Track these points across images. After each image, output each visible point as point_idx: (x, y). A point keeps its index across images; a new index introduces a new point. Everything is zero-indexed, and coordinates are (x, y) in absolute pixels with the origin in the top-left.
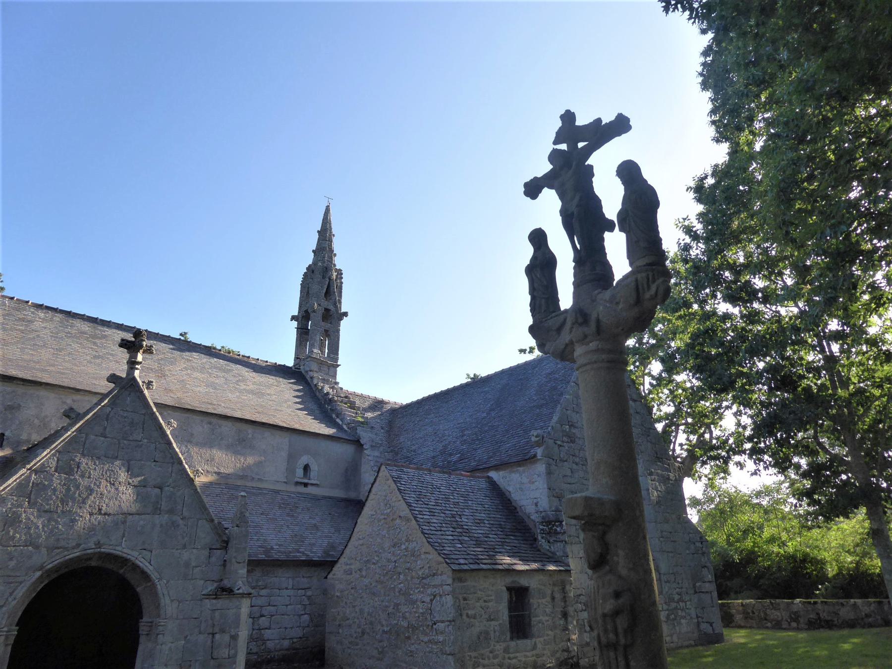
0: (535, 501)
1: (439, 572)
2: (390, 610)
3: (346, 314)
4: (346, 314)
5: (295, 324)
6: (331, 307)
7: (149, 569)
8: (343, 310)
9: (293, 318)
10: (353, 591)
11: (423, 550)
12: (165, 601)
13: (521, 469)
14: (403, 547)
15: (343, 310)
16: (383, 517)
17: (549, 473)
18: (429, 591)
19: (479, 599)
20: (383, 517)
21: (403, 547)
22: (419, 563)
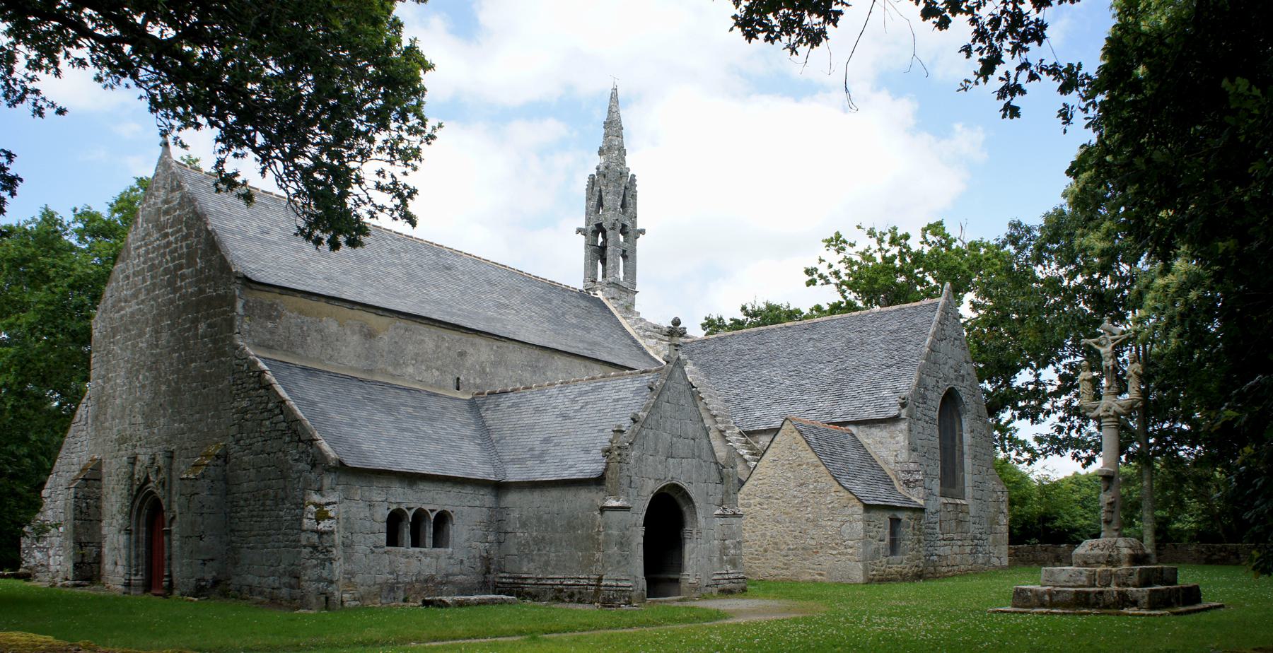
0: (895, 453)
1: (850, 505)
2: (797, 533)
3: (642, 232)
4: (642, 232)
5: (581, 239)
6: (628, 223)
7: (693, 496)
8: (639, 227)
9: (579, 231)
10: (752, 520)
11: (833, 489)
12: (700, 517)
13: (882, 425)
14: (811, 486)
15: (639, 227)
16: (787, 462)
17: (910, 430)
18: (839, 519)
19: (875, 526)
20: (787, 462)
21: (811, 486)
22: (828, 498)
